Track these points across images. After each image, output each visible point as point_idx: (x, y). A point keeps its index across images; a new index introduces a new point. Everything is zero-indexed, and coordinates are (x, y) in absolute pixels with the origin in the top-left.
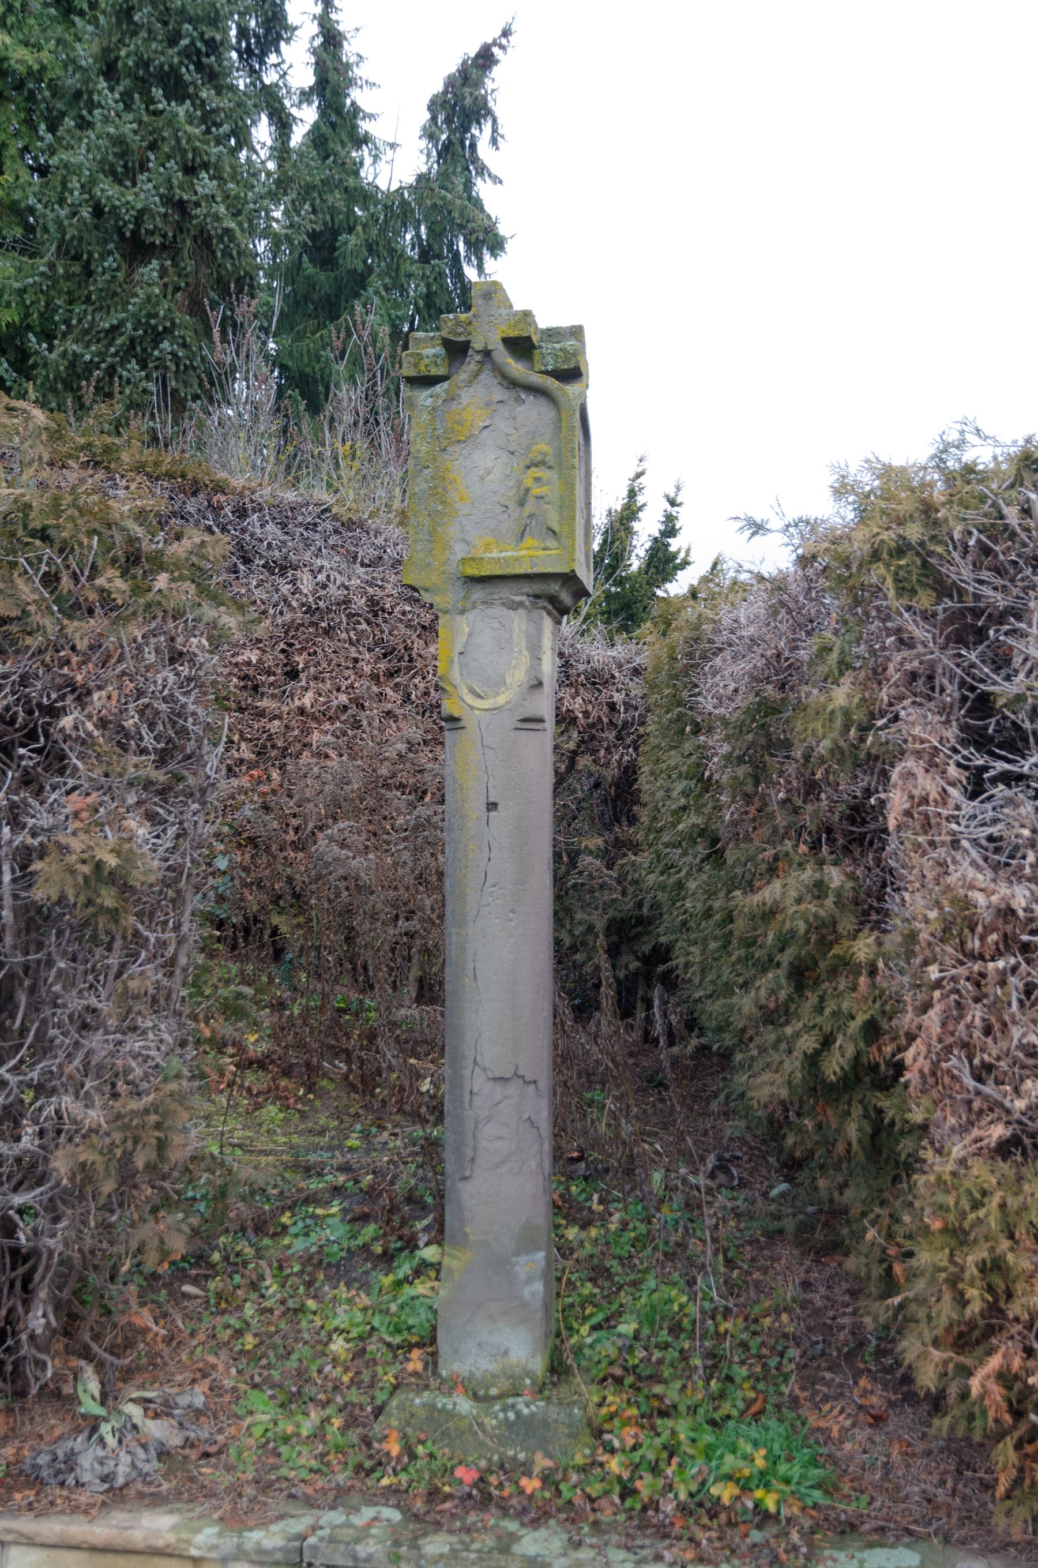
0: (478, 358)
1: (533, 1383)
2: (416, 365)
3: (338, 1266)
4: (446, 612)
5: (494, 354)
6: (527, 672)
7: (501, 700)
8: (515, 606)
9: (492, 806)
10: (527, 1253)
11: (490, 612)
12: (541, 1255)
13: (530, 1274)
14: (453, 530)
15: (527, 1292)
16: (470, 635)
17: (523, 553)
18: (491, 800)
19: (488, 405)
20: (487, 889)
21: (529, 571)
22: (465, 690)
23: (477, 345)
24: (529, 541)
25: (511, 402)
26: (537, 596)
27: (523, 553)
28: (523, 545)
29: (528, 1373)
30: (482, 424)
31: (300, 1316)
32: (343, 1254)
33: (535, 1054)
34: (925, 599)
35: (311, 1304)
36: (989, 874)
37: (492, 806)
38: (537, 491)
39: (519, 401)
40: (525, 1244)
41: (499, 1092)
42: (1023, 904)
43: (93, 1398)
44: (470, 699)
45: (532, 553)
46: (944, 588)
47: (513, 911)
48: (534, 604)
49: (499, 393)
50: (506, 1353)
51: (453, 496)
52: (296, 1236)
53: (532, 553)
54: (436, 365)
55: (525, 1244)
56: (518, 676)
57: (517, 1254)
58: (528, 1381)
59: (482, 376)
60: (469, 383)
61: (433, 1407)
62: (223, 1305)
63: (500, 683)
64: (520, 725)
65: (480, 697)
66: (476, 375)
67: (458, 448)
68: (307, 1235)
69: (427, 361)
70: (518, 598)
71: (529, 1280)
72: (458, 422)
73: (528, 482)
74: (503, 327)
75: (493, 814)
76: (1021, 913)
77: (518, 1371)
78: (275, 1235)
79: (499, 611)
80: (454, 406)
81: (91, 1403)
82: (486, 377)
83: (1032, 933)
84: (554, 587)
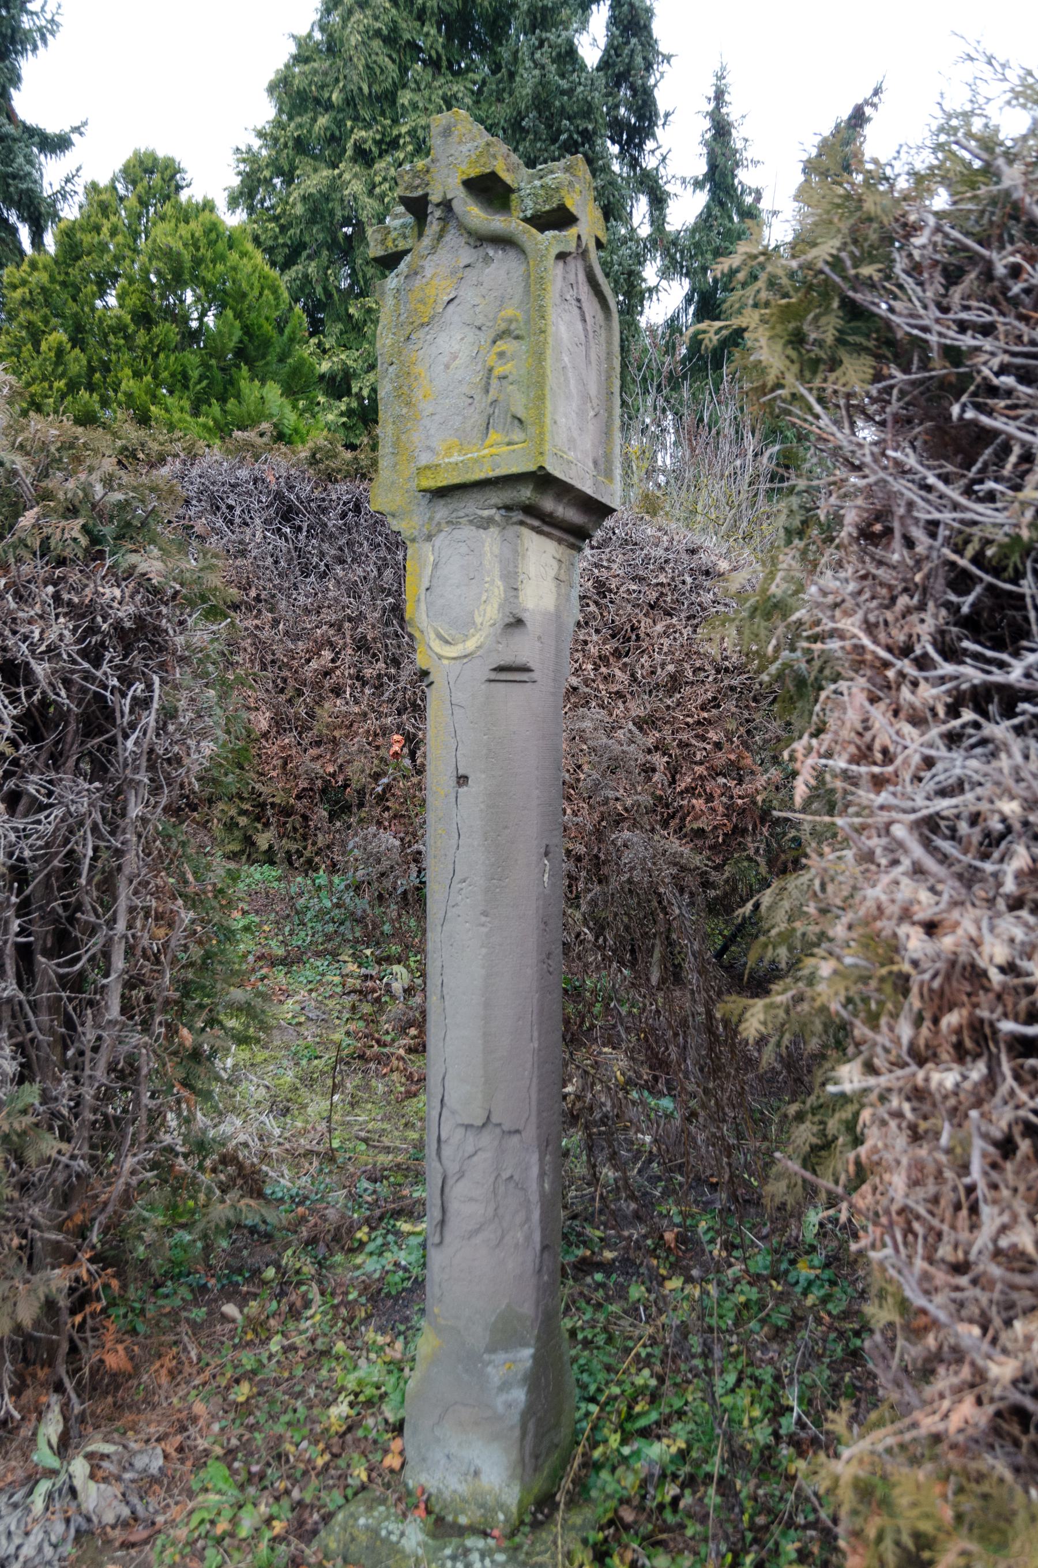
0: (438, 213)
1: (507, 1520)
2: (383, 242)
3: (396, 1298)
4: (413, 540)
5: (455, 204)
6: (501, 606)
7: (471, 645)
8: (485, 524)
9: (462, 780)
10: (506, 1350)
11: (458, 534)
12: (527, 1353)
13: (507, 1378)
14: (417, 438)
15: (499, 1402)
16: (436, 565)
17: (486, 452)
18: (461, 772)
19: (453, 273)
20: (456, 886)
21: (491, 474)
22: (432, 636)
23: (435, 198)
24: (494, 436)
25: (479, 265)
26: (508, 508)
27: (486, 452)
28: (488, 442)
29: (502, 1506)
30: (446, 298)
31: (324, 1360)
32: (408, 1284)
33: (520, 1098)
34: (854, 374)
35: (340, 1347)
36: (949, 889)
37: (462, 780)
38: (499, 371)
39: (487, 260)
40: (503, 1337)
41: (471, 1143)
42: (1001, 958)
43: (51, 1447)
44: (437, 646)
45: (493, 450)
46: (891, 347)
47: (485, 914)
48: (507, 518)
49: (467, 255)
50: (476, 1473)
51: (418, 394)
52: (371, 1254)
53: (493, 450)
54: (405, 237)
55: (503, 1337)
56: (490, 613)
57: (492, 1349)
58: (501, 1517)
59: (447, 238)
60: (434, 249)
61: (374, 1532)
62: (250, 1336)
63: (468, 624)
64: (494, 676)
65: (447, 642)
66: (440, 236)
67: (421, 334)
68: (380, 1254)
69: (394, 234)
70: (486, 513)
71: (505, 1386)
72: (422, 301)
73: (492, 359)
74: (463, 167)
75: (463, 790)
76: (996, 977)
77: (490, 1500)
78: (351, 1250)
79: (467, 532)
80: (418, 282)
81: (48, 1451)
82: (452, 238)
83: (1032, 1017)
84: (526, 493)
